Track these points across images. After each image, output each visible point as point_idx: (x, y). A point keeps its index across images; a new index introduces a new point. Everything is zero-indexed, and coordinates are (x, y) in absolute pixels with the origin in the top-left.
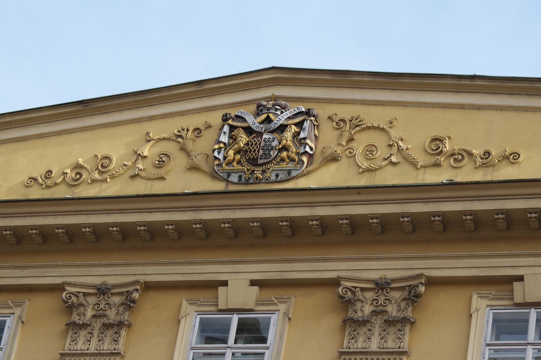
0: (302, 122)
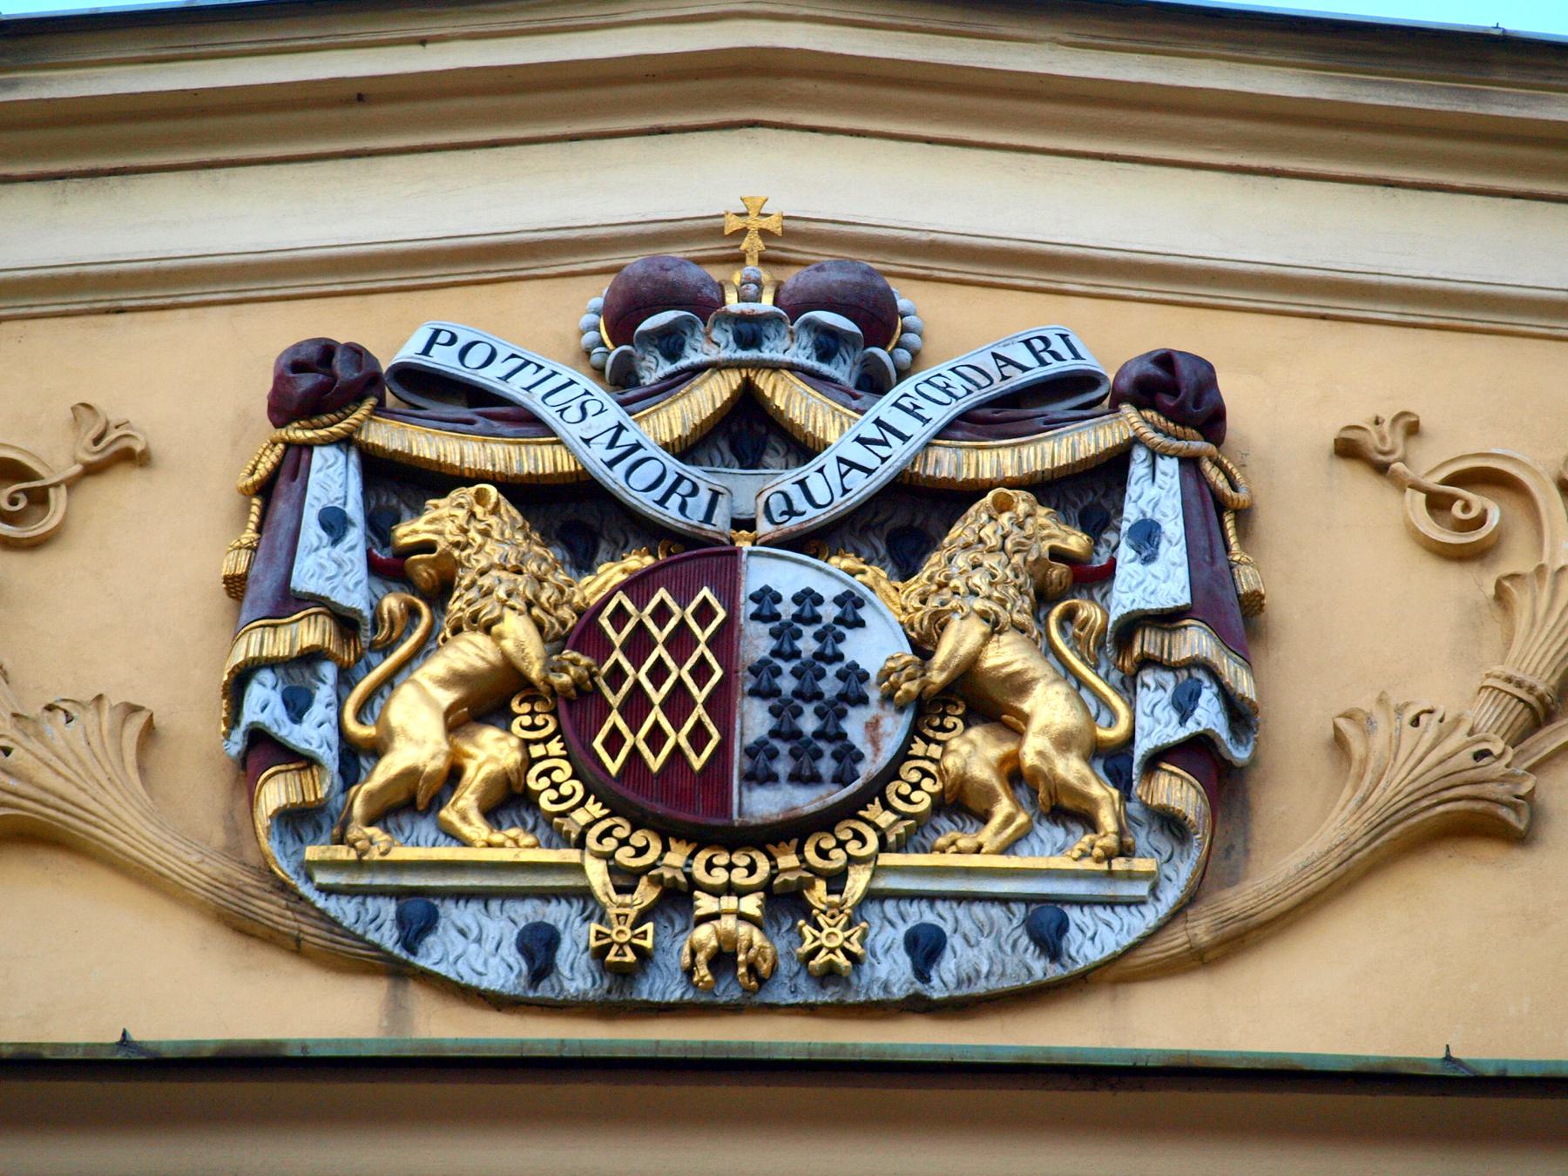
0: (1110, 470)
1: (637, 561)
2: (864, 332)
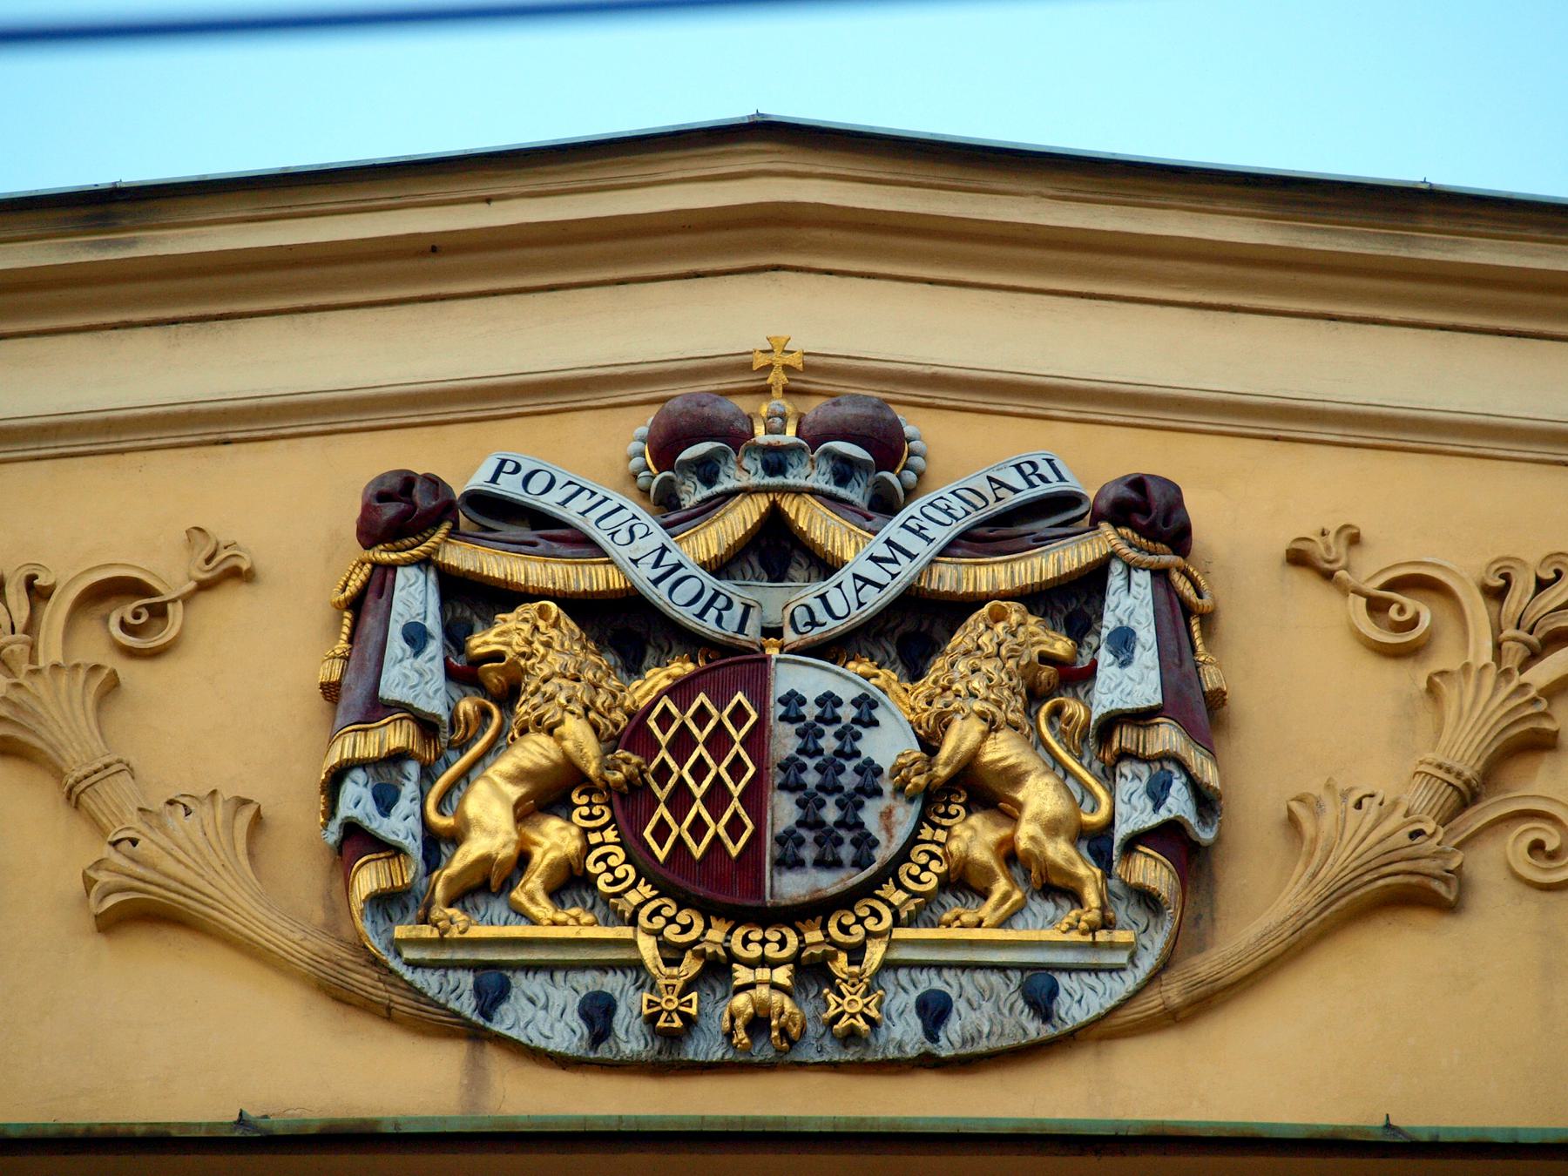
0: (1092, 581)
1: (681, 668)
2: (876, 464)
